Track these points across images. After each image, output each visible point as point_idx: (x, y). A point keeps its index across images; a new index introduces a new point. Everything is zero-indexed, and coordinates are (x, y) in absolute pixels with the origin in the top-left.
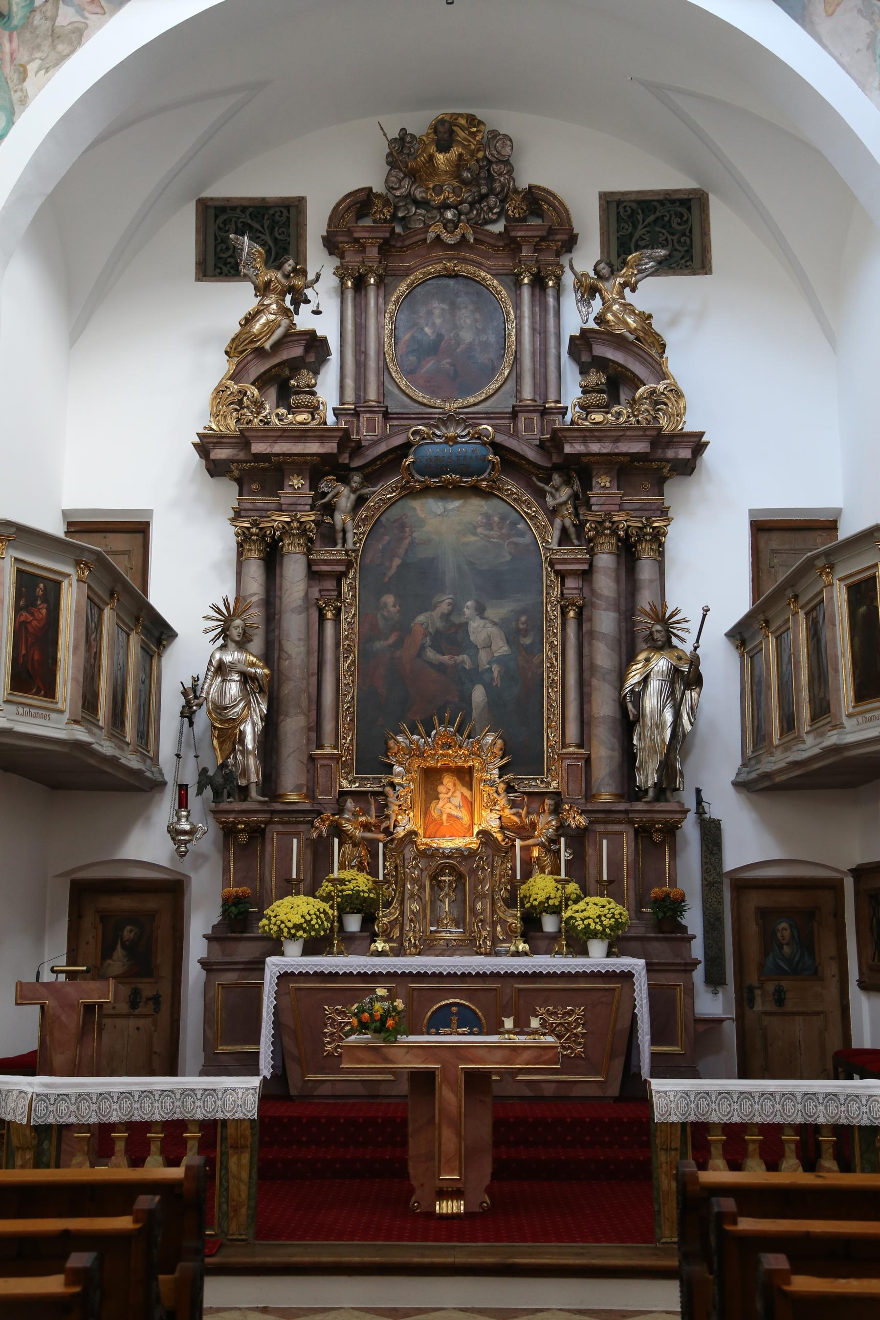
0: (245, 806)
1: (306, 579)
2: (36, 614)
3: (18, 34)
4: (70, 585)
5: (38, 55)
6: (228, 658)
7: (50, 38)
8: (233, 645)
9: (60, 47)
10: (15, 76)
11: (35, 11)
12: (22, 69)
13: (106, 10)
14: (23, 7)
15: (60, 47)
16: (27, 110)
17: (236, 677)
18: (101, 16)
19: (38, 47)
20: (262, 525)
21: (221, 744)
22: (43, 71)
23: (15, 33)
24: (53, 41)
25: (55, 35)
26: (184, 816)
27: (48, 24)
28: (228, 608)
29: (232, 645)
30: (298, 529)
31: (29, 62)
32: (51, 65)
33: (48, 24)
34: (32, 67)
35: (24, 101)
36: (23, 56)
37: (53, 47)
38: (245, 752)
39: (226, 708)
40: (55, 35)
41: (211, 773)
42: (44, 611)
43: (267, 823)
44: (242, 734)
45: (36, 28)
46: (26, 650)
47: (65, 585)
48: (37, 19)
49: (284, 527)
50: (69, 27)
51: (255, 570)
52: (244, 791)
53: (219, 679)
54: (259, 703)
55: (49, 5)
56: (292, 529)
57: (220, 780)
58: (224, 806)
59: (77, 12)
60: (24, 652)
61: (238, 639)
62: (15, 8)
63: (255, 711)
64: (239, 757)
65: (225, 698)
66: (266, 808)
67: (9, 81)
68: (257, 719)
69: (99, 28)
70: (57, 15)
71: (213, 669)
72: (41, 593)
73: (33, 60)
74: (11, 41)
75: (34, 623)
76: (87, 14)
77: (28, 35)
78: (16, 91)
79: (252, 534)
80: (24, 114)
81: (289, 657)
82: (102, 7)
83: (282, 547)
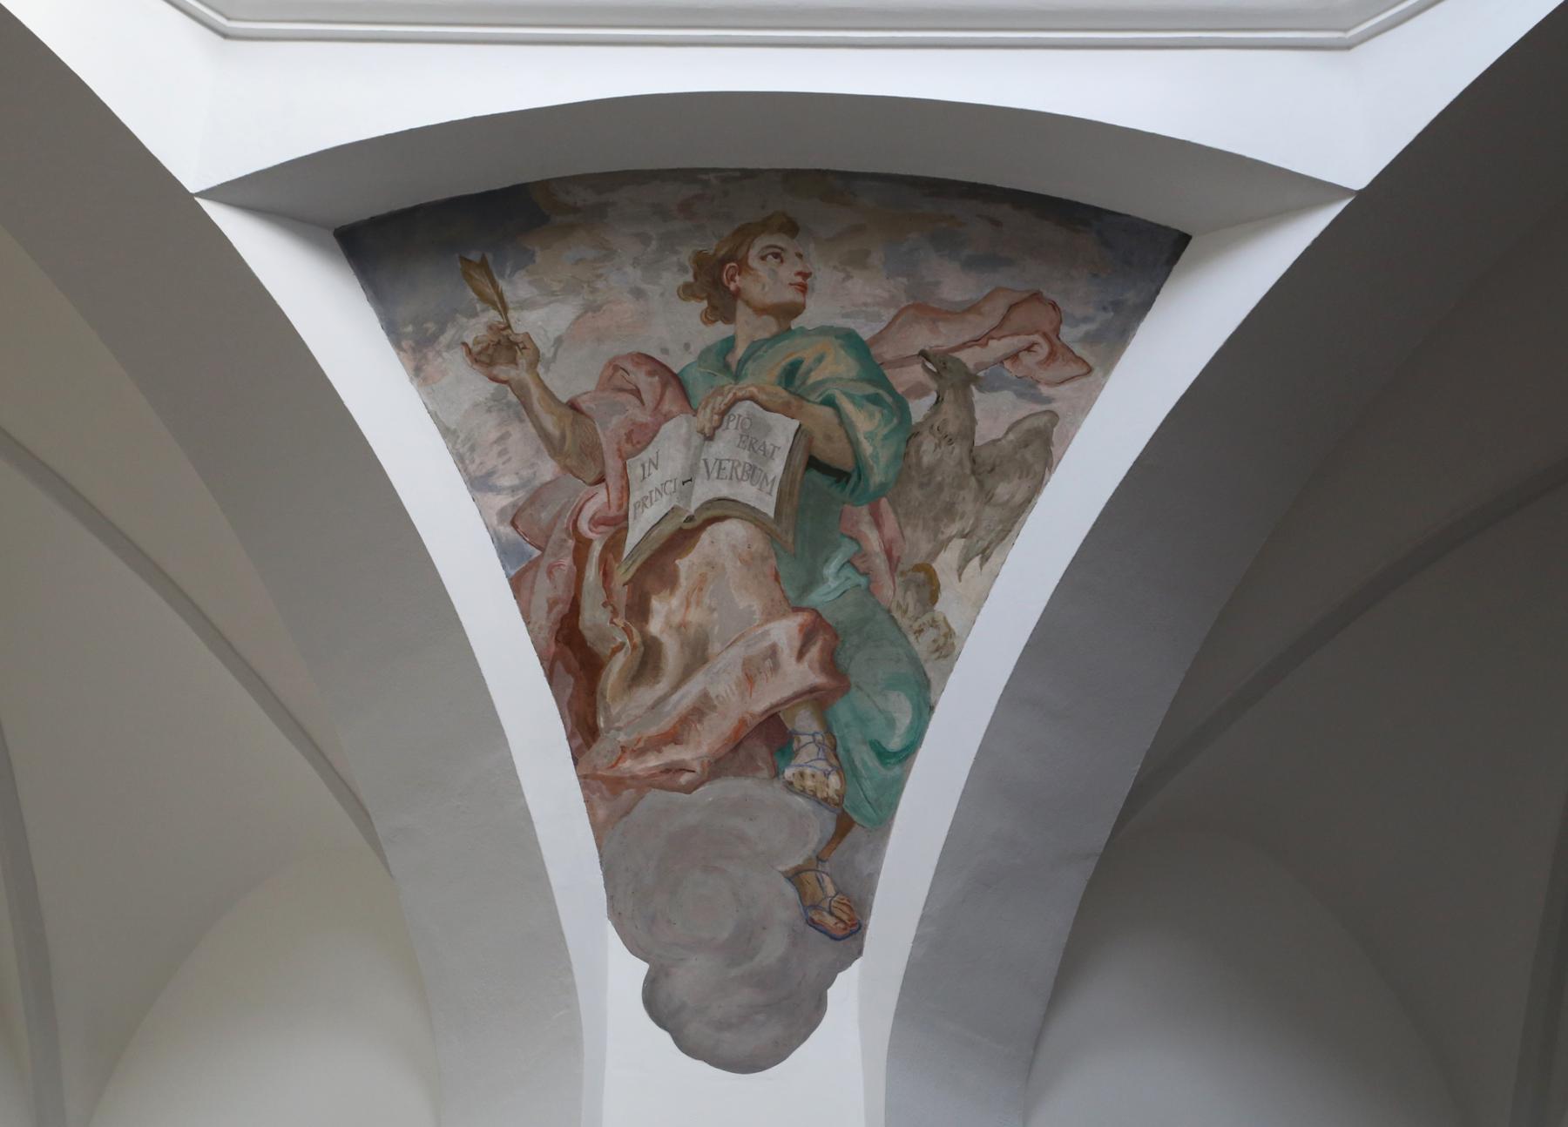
3: (892, 503)
5: (954, 528)
7: (973, 481)
9: (1003, 490)
10: (911, 598)
11: (917, 434)
12: (922, 575)
13: (1091, 360)
14: (885, 437)
15: (1003, 490)
16: (957, 666)
18: (1084, 380)
19: (950, 511)
22: (976, 561)
23: (884, 502)
24: (981, 483)
25: (983, 469)
27: (958, 450)
31: (934, 554)
32: (990, 542)
33: (958, 450)
34: (945, 563)
35: (947, 648)
36: (917, 543)
37: (985, 495)
40: (983, 469)
45: (931, 470)
48: (928, 450)
50: (1011, 437)
55: (948, 409)
59: (1020, 395)
62: (867, 448)
67: (897, 615)
69: (1086, 410)
70: (973, 421)
73: (943, 545)
74: (877, 523)
76: (1045, 390)
77: (916, 494)
78: (920, 631)
80: (952, 677)
82: (1079, 360)
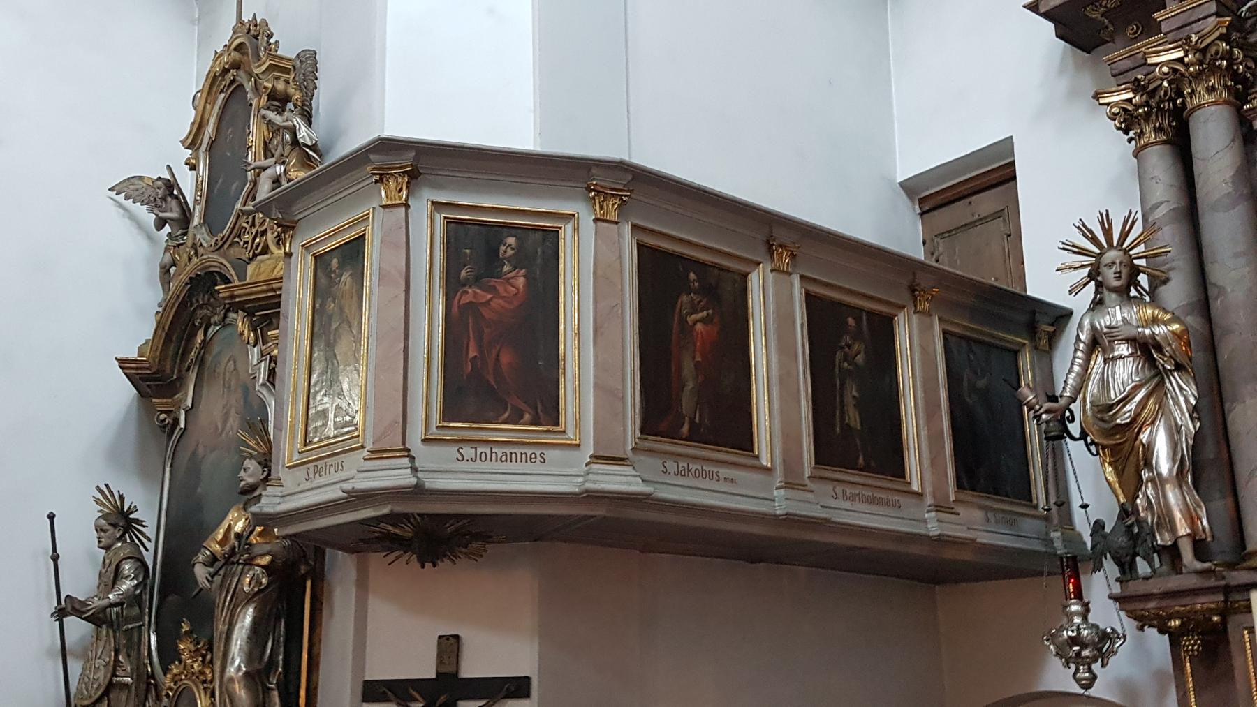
0: (1175, 582)
1: (1238, 144)
2: (500, 289)
4: (576, 230)
6: (1104, 321)
8: (1114, 296)
17: (1123, 349)
20: (1151, 87)
21: (1119, 473)
26: (1076, 613)
28: (1094, 240)
29: (1110, 297)
30: (1200, 63)
38: (1158, 481)
39: (1111, 407)
41: (1108, 530)
42: (521, 281)
43: (1225, 613)
44: (1149, 449)
46: (480, 348)
47: (567, 230)
49: (1175, 71)
51: (1160, 162)
52: (1173, 552)
53: (1100, 359)
54: (1181, 389)
56: (1187, 66)
57: (1122, 540)
58: (1136, 588)
60: (472, 354)
61: (1116, 284)
63: (1177, 403)
64: (1150, 492)
65: (1109, 391)
66: (1212, 582)
68: (1182, 416)
71: (1082, 345)
72: (510, 252)
75: (496, 303)
79: (1137, 107)
81: (1222, 291)
83: (1183, 103)
